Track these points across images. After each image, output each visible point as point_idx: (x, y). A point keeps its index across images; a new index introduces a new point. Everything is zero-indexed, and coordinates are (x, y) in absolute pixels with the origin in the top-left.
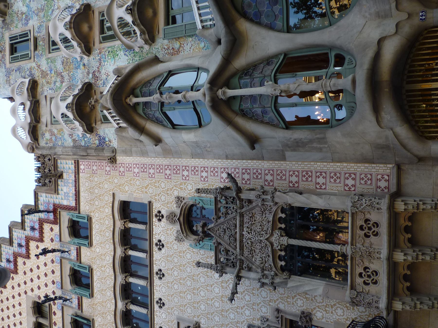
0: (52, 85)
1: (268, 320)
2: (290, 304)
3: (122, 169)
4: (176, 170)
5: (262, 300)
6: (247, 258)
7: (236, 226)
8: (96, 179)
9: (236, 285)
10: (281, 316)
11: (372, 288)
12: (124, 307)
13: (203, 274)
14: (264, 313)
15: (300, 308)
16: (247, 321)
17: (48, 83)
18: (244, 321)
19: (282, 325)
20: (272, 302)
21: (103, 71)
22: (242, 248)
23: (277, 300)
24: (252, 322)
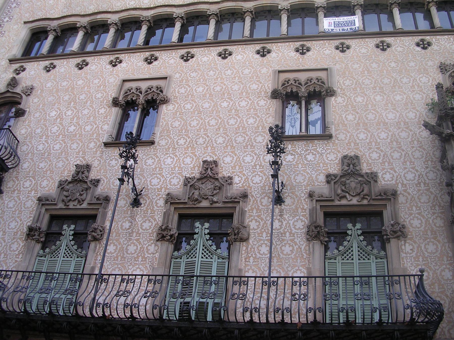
1: (376, 181)
2: (409, 210)
5: (400, 174)
10: (390, 199)
12: (320, 5)
13: (407, 98)
14: (382, 176)
15: (408, 223)
16: (362, 156)
18: (361, 151)
19: (374, 199)
20: (402, 187)
23: (409, 194)
24: (363, 161)
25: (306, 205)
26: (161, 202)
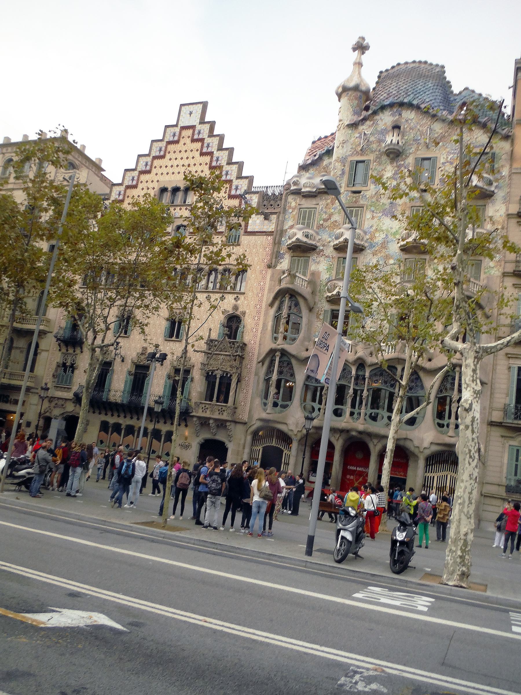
0: (324, 210)
3: (264, 272)
4: (259, 312)
6: (212, 356)
7: (226, 352)
8: (261, 250)
9: (201, 352)
11: (201, 410)
17: (327, 205)
21: (322, 259)
22: (216, 354)
25: (169, 367)
26: (130, 361)
